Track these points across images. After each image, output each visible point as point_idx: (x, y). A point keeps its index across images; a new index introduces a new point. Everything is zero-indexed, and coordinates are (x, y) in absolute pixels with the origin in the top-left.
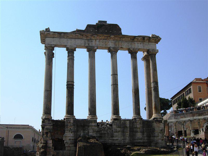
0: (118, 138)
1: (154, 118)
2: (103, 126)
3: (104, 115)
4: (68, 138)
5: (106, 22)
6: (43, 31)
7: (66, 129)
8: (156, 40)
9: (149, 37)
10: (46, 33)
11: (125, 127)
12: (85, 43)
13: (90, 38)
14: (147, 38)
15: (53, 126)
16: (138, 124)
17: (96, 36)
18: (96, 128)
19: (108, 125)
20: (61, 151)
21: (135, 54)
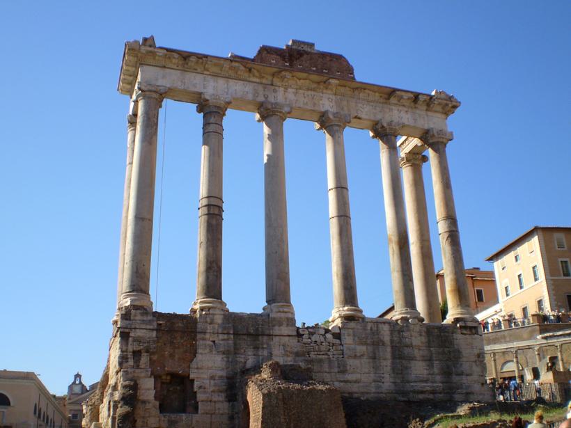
0: (365, 377)
1: (457, 320)
2: (314, 338)
3: (316, 305)
4: (205, 375)
5: (313, 45)
6: (136, 42)
7: (201, 342)
8: (447, 105)
9: (431, 97)
10: (144, 49)
11: (378, 344)
12: (256, 94)
13: (270, 83)
14: (425, 97)
15: (157, 330)
16: (414, 334)
17: (288, 75)
18: (294, 341)
19: (329, 336)
20: (184, 416)
21: (393, 138)
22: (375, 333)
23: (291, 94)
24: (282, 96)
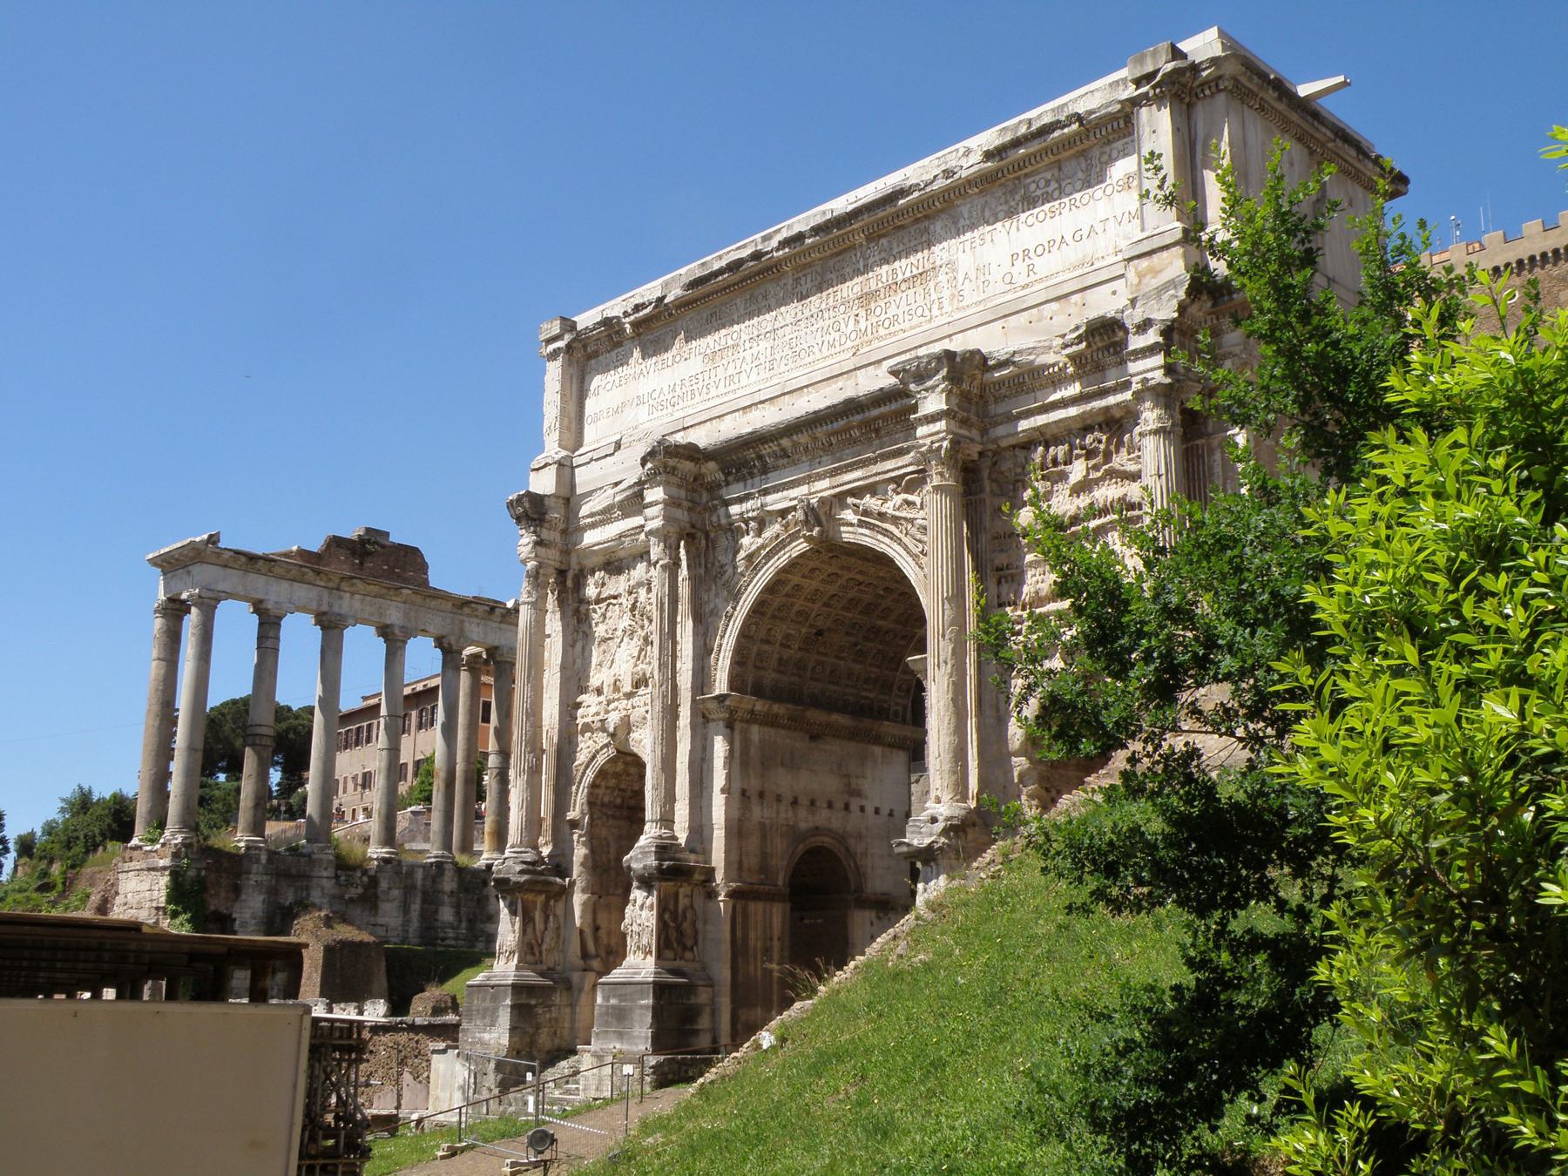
24: (347, 603)
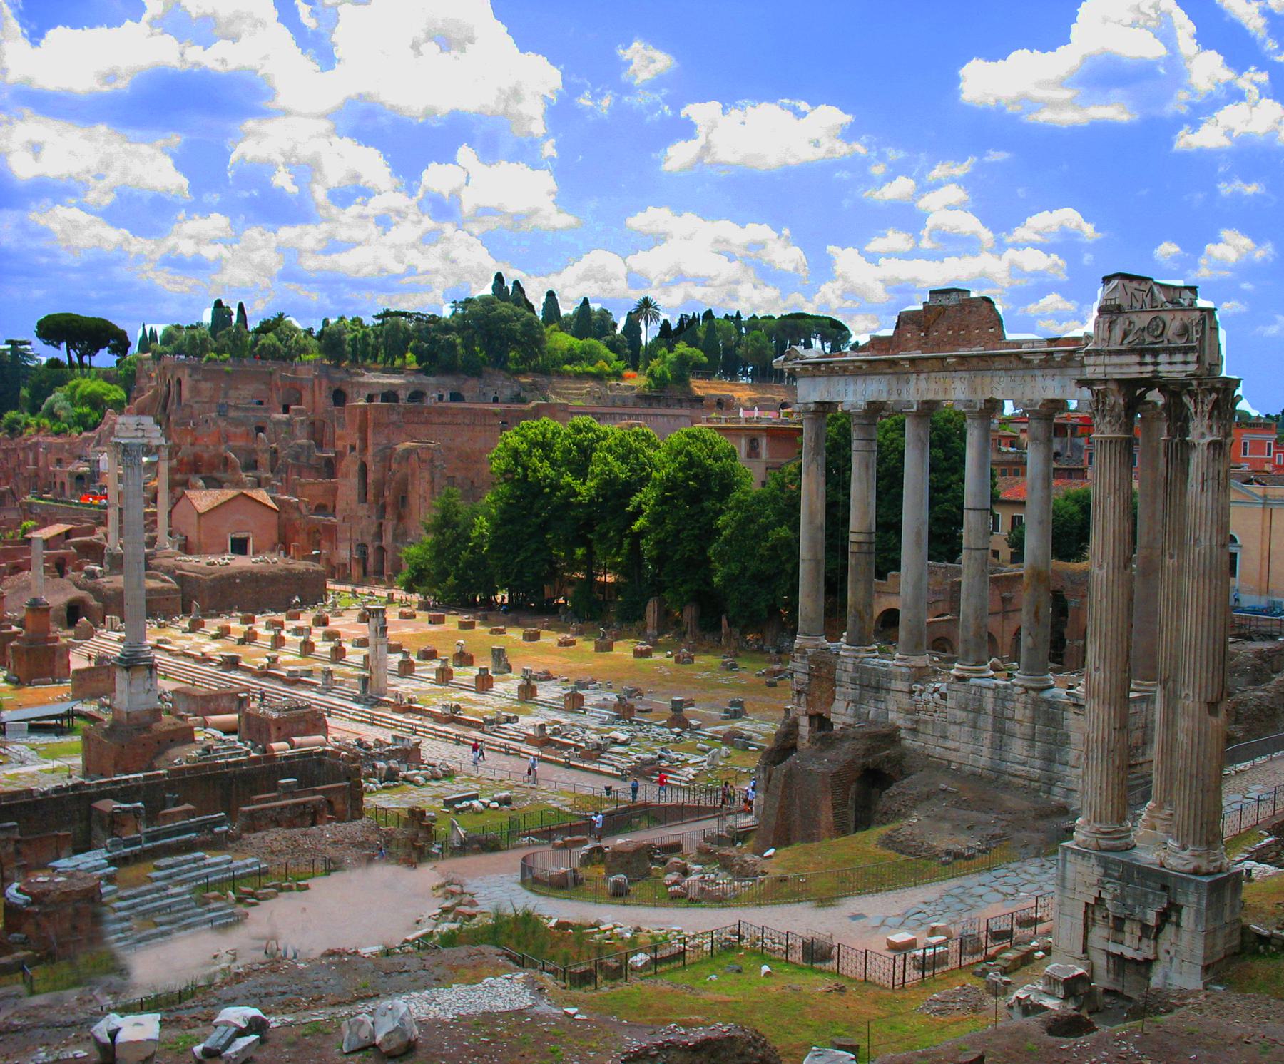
11: (979, 711)
22: (980, 699)
23: (923, 385)
